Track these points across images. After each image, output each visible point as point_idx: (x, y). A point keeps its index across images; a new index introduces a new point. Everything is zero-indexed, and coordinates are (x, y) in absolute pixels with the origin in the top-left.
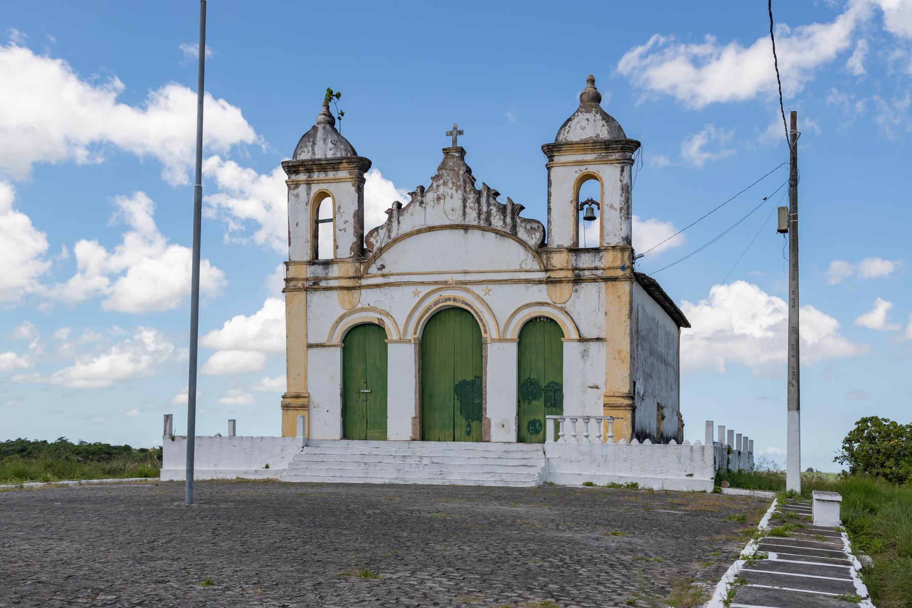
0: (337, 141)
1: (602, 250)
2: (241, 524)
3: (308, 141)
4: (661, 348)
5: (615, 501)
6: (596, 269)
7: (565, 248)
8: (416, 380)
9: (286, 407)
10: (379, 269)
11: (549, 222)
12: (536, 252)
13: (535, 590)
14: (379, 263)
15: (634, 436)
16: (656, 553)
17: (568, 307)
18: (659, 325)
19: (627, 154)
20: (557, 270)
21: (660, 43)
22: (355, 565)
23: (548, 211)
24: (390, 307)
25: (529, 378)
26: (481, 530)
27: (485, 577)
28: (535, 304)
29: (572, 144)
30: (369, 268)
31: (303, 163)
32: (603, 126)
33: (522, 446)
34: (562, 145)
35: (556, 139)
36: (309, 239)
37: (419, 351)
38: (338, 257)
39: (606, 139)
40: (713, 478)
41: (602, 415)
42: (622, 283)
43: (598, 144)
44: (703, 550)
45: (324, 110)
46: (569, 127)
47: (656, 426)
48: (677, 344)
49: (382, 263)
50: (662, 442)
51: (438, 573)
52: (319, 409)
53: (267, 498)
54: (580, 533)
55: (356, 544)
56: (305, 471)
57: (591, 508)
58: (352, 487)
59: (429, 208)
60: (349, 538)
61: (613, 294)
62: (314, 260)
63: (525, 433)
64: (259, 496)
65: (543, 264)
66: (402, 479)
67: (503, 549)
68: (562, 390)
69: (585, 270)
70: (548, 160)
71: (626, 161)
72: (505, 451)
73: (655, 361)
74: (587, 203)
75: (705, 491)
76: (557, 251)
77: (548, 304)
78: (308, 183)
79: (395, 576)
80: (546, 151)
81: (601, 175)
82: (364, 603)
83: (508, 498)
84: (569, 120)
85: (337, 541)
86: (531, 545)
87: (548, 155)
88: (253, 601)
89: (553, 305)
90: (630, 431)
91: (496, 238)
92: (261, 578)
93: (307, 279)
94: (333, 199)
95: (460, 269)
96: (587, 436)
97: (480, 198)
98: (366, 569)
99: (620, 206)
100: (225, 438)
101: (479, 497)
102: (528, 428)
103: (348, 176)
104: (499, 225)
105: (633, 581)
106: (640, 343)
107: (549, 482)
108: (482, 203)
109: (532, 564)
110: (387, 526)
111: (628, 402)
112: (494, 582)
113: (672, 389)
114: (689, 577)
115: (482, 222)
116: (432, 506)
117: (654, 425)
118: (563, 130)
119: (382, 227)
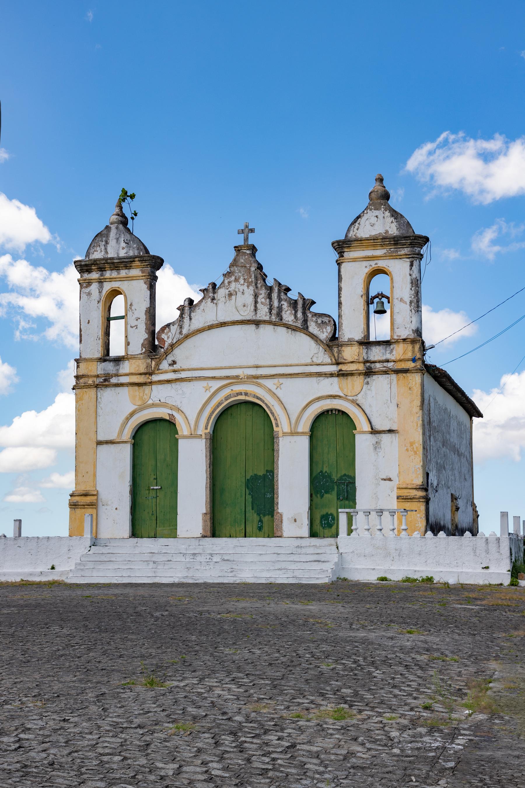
0: (129, 240)
1: (393, 342)
2: (23, 630)
4: (454, 439)
5: (410, 597)
6: (387, 361)
9: (74, 505)
10: (170, 365)
11: (340, 316)
12: (327, 345)
13: (327, 696)
14: (170, 359)
15: (428, 529)
16: (452, 652)
17: (360, 399)
18: (451, 416)
19: (416, 249)
20: (348, 363)
21: (450, 140)
22: (141, 673)
23: (339, 306)
25: (321, 472)
26: (273, 631)
27: (276, 683)
30: (160, 363)
31: (95, 262)
32: (392, 222)
33: (315, 541)
34: (352, 241)
35: (346, 236)
36: (100, 336)
37: (210, 446)
38: (129, 353)
40: (509, 571)
41: (396, 508)
42: (413, 375)
43: (388, 240)
44: (501, 648)
45: (117, 210)
46: (359, 224)
47: (450, 518)
48: (470, 434)
49: (173, 359)
50: (457, 534)
51: (227, 680)
52: (108, 507)
53: (51, 602)
54: (375, 632)
55: (142, 650)
56: (92, 571)
57: (385, 604)
58: (140, 588)
59: (221, 305)
60: (135, 643)
61: (405, 386)
62: (105, 357)
63: (318, 528)
64: (43, 600)
65: (334, 357)
66: (192, 578)
67: (295, 651)
68: (355, 483)
69: (376, 362)
70: (338, 256)
71: (415, 256)
72: (298, 547)
73: (448, 451)
74: (378, 297)
75: (501, 584)
76: (349, 345)
77: (340, 397)
78: (101, 282)
79: (182, 684)
80: (336, 247)
81: (391, 269)
82: (149, 714)
83: (301, 595)
84: (359, 217)
85: (122, 646)
86: (323, 646)
87: (339, 251)
88: (32, 716)
89: (345, 398)
90: (424, 523)
91: (288, 332)
92: (42, 690)
93: (98, 376)
94: (125, 297)
95: (252, 363)
96: (381, 530)
97: (272, 293)
98: (152, 676)
99: (410, 299)
100: (10, 538)
101: (271, 596)
102: (321, 522)
103: (140, 274)
104: (290, 320)
105: (429, 683)
106: (433, 434)
107: (342, 577)
108: (273, 299)
109: (324, 667)
110: (175, 629)
111: (421, 493)
112: (285, 688)
113: (465, 479)
114: (487, 677)
115: (274, 318)
116: (222, 607)
117: (448, 516)
118: (353, 227)
119: (173, 323)
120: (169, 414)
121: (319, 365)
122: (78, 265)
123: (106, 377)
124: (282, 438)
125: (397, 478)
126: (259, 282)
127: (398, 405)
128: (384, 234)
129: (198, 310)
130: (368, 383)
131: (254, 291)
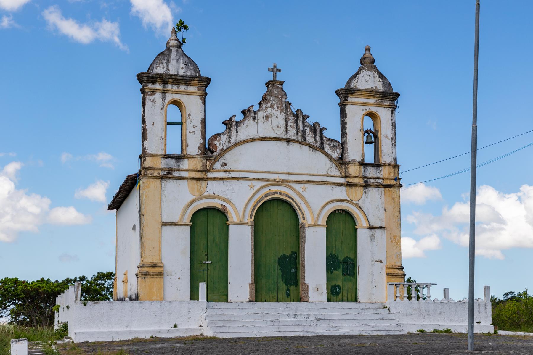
0: (187, 62)
1: (382, 165)
3: (163, 59)
6: (378, 178)
7: (358, 162)
8: (252, 254)
9: (144, 275)
10: (222, 166)
14: (222, 161)
17: (360, 203)
20: (353, 177)
24: (231, 196)
28: (339, 200)
29: (359, 90)
31: (161, 76)
32: (379, 81)
39: (381, 90)
42: (395, 189)
46: (358, 78)
49: (224, 161)
59: (260, 123)
61: (390, 197)
76: (353, 164)
77: (348, 201)
78: (164, 93)
87: (344, 96)
91: (310, 150)
93: (162, 170)
95: (285, 170)
99: (392, 137)
103: (196, 91)
104: (311, 142)
108: (299, 124)
115: (300, 138)
118: (354, 80)
121: (333, 176)
122: (146, 76)
123: (169, 170)
124: (307, 228)
125: (386, 261)
126: (289, 110)
127: (385, 210)
128: (374, 89)
129: (243, 126)
130: (365, 193)
131: (285, 116)
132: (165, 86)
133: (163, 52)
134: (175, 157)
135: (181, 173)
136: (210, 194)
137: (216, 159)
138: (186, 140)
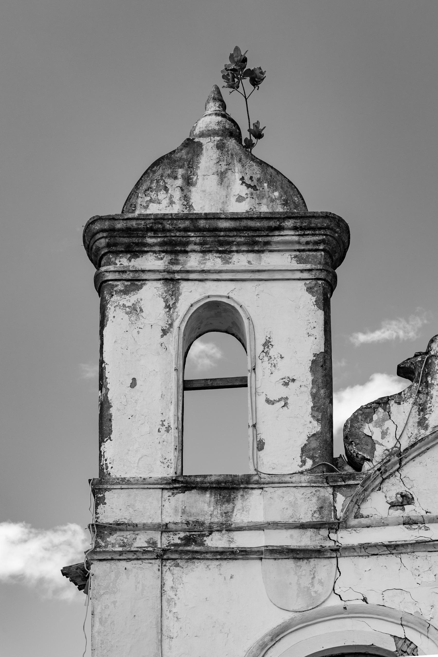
3: (169, 176)
120: (395, 637)
132: (177, 260)
133: (171, 153)
134: (212, 483)
135: (235, 538)
136: (348, 603)
137: (368, 482)
138: (254, 426)
